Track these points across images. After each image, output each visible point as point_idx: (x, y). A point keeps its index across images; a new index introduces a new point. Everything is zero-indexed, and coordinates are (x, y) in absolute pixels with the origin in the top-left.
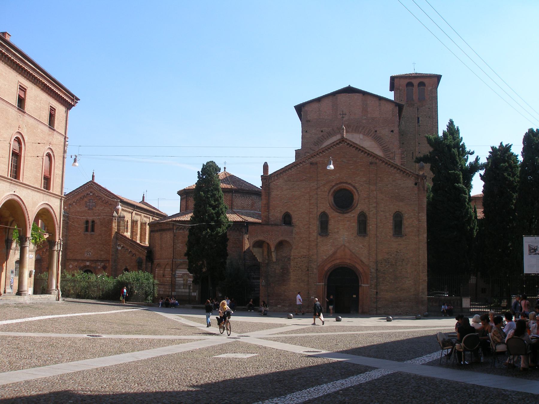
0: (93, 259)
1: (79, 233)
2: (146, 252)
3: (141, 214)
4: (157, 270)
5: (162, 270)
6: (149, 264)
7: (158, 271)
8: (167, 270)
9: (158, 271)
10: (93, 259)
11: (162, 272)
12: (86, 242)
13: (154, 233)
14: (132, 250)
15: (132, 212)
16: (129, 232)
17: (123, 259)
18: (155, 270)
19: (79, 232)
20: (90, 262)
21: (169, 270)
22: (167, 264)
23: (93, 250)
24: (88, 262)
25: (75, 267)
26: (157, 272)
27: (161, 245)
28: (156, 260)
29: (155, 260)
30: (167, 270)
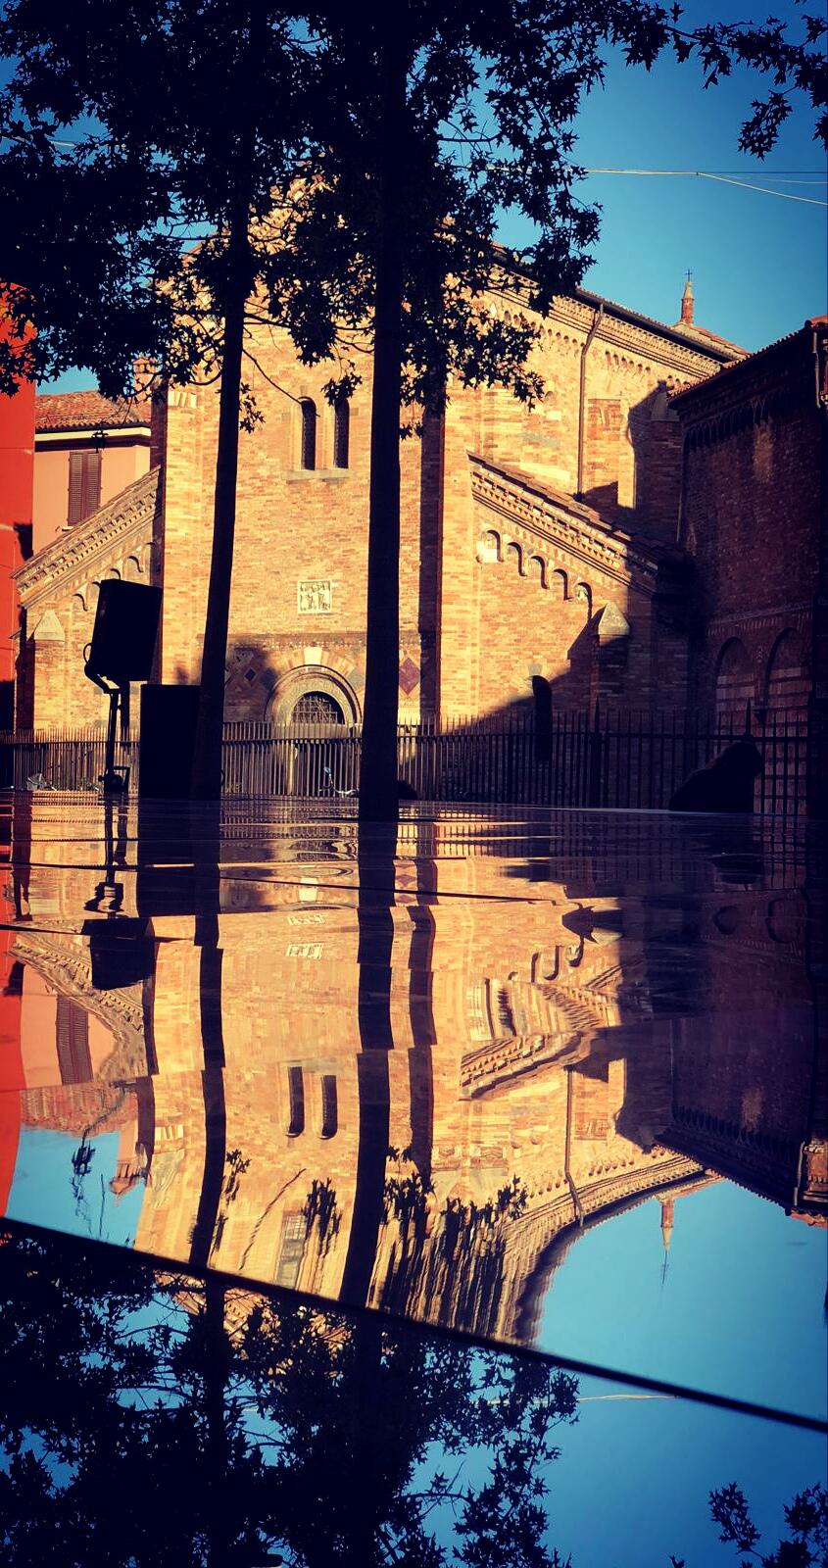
0: (336, 628)
1: (261, 479)
2: (650, 571)
3: (646, 362)
4: (722, 680)
5: (751, 678)
6: (678, 649)
7: (729, 686)
8: (781, 673)
9: (729, 686)
10: (344, 630)
11: (750, 691)
12: (303, 530)
13: (706, 451)
14: (567, 562)
15: (585, 347)
16: (565, 465)
17: (513, 620)
18: (715, 685)
19: (263, 472)
20: (325, 648)
21: (795, 672)
22: (785, 633)
23: (338, 574)
24: (314, 645)
25: (246, 681)
26: (722, 694)
27: (744, 517)
28: (717, 622)
29: (712, 617)
30: (781, 673)
